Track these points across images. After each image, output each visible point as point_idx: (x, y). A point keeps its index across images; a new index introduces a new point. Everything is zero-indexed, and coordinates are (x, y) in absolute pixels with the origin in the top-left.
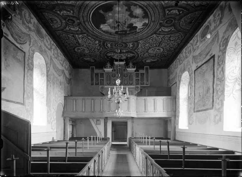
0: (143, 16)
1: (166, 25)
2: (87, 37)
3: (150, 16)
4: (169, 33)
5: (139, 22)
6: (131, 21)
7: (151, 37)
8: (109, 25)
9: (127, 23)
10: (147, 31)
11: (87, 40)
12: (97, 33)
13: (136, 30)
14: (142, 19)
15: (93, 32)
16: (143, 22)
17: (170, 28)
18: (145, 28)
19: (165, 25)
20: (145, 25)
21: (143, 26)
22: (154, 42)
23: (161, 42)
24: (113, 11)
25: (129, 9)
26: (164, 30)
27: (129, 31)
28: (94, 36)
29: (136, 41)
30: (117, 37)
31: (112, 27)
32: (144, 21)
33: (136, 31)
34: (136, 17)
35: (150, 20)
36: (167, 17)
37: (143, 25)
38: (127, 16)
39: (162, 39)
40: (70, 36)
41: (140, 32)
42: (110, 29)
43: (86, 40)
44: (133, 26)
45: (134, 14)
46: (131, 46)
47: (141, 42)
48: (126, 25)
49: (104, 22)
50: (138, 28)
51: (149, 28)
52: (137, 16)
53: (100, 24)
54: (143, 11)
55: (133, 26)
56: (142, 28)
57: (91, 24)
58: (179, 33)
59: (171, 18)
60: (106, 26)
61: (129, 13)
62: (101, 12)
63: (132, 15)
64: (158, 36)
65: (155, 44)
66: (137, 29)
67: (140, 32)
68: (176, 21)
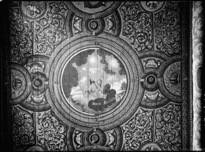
0: (119, 70)
1: (149, 86)
2: (50, 116)
3: (127, 71)
4: (158, 103)
5: (117, 81)
6: (108, 80)
7: (135, 114)
8: (81, 89)
9: (102, 83)
10: (128, 99)
11: (49, 125)
12: (65, 107)
13: (115, 97)
14: (119, 75)
15: (60, 105)
16: (122, 82)
17: (154, 92)
18: (126, 92)
19: (149, 87)
20: (125, 86)
21: (122, 89)
22: (142, 127)
23: (152, 126)
24: (87, 64)
25: (104, 61)
26: (149, 97)
27: (107, 99)
28: (60, 113)
29: (118, 127)
30: (92, 113)
31: (85, 92)
32: (122, 79)
33: (115, 100)
34: (112, 73)
35: (128, 77)
36: (147, 71)
37: (121, 87)
38: (102, 71)
39: (152, 118)
40: (28, 116)
41: (120, 102)
42: (82, 96)
43: (47, 124)
44: (110, 89)
45: (110, 69)
46: (112, 139)
47: (124, 129)
48: (102, 89)
49: (76, 85)
50: (118, 92)
51: (131, 91)
52: (113, 71)
53: (71, 88)
54: (118, 62)
55: (110, 89)
56: (122, 94)
57: (61, 87)
58: (170, 104)
59: (151, 73)
60: (78, 90)
61: (104, 66)
62: (74, 65)
63: (108, 71)
64: (145, 112)
65: (146, 133)
66: (116, 95)
67: (120, 102)
68: (159, 80)
